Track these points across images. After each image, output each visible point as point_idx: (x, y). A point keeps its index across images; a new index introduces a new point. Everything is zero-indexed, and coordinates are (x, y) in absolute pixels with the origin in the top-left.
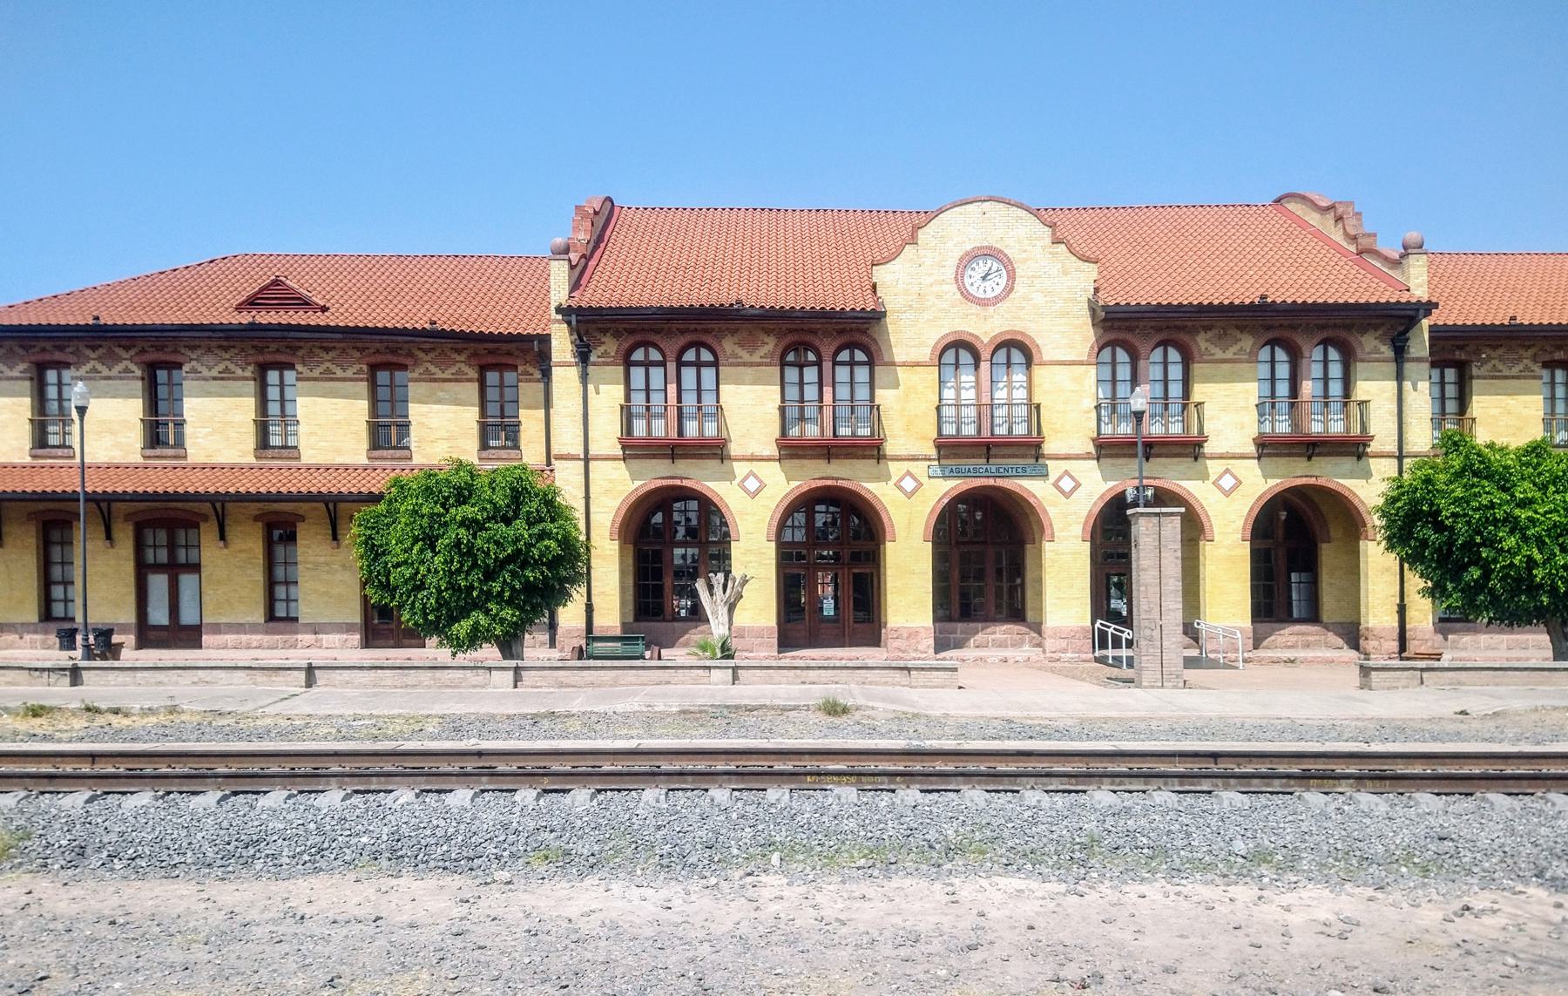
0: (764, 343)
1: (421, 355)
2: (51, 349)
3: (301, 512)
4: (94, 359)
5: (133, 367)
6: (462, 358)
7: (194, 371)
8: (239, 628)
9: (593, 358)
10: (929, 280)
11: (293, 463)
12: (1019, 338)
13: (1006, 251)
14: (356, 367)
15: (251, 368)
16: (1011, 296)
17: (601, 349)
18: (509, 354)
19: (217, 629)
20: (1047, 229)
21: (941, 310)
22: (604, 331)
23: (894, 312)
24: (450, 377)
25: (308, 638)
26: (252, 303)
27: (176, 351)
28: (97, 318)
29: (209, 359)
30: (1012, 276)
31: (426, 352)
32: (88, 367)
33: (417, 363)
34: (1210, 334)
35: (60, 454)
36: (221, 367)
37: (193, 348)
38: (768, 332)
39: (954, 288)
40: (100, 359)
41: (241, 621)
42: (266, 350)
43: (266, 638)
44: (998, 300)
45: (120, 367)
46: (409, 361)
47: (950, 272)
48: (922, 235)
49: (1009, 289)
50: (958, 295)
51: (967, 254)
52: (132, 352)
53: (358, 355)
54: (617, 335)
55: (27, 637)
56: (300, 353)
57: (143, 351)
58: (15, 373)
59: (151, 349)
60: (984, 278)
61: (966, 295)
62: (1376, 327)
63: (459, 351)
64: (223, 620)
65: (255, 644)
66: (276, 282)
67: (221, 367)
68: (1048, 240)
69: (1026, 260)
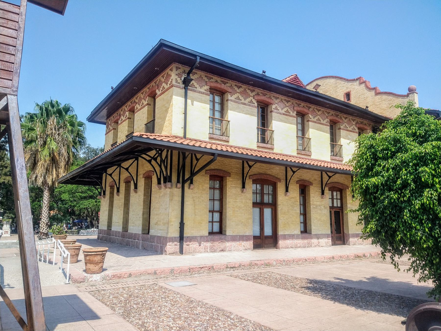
2: (220, 82)
3: (311, 181)
4: (239, 93)
5: (254, 101)
7: (276, 108)
8: (292, 237)
11: (309, 158)
14: (327, 120)
15: (295, 112)
18: (365, 124)
19: (285, 237)
24: (351, 130)
25: (314, 241)
27: (270, 98)
29: (282, 105)
35: (224, 139)
41: (293, 234)
42: (300, 106)
43: (300, 242)
45: (249, 100)
52: (254, 93)
53: (327, 115)
55: (204, 244)
56: (311, 109)
57: (258, 94)
58: (202, 90)
59: (261, 94)
63: (354, 120)
64: (287, 233)
65: (299, 245)
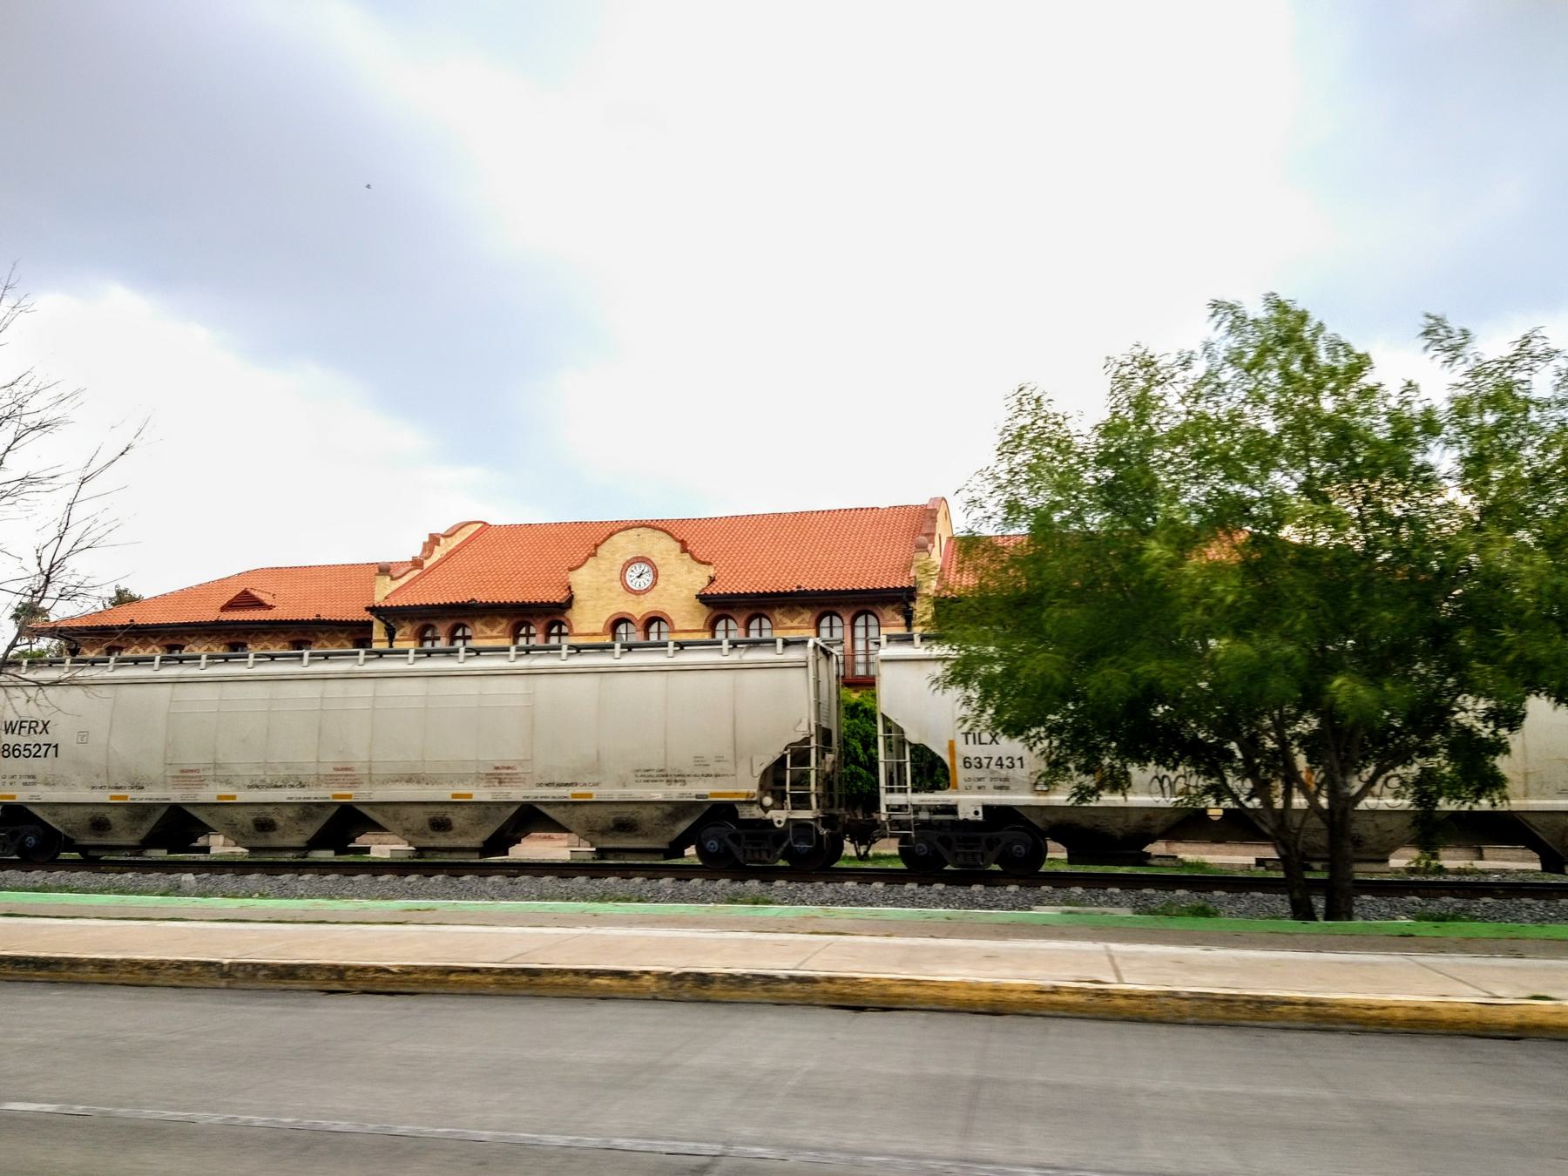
0: (500, 623)
1: (320, 635)
6: (345, 635)
9: (397, 637)
10: (604, 579)
12: (616, 617)
13: (652, 559)
16: (656, 588)
17: (402, 631)
20: (678, 544)
21: (610, 599)
22: (404, 619)
23: (581, 601)
26: (230, 606)
27: (182, 638)
28: (132, 621)
29: (199, 642)
30: (656, 575)
31: (323, 632)
32: (134, 648)
33: (317, 641)
34: (782, 610)
36: (206, 647)
37: (191, 636)
38: (503, 616)
39: (619, 584)
40: (139, 645)
44: (647, 590)
46: (312, 639)
47: (616, 574)
48: (602, 551)
49: (654, 584)
50: (622, 589)
51: (628, 562)
54: (412, 620)
57: (164, 639)
60: (639, 577)
61: (628, 589)
62: (893, 603)
63: (342, 632)
66: (245, 592)
67: (206, 647)
68: (678, 551)
69: (664, 565)
